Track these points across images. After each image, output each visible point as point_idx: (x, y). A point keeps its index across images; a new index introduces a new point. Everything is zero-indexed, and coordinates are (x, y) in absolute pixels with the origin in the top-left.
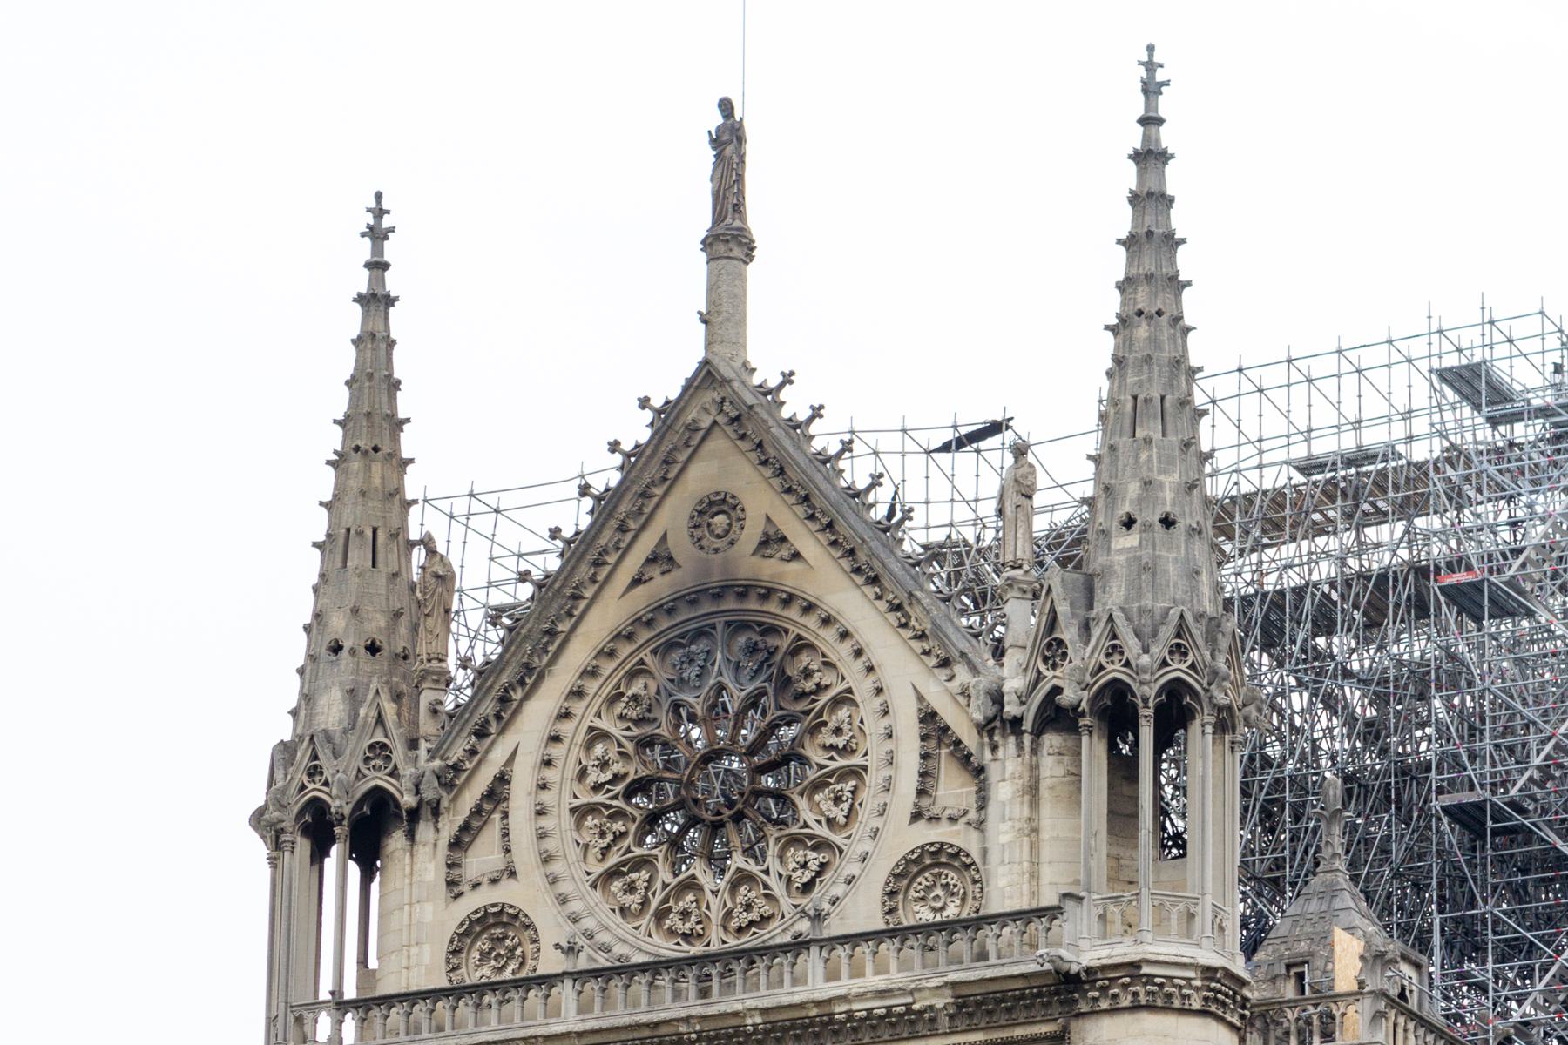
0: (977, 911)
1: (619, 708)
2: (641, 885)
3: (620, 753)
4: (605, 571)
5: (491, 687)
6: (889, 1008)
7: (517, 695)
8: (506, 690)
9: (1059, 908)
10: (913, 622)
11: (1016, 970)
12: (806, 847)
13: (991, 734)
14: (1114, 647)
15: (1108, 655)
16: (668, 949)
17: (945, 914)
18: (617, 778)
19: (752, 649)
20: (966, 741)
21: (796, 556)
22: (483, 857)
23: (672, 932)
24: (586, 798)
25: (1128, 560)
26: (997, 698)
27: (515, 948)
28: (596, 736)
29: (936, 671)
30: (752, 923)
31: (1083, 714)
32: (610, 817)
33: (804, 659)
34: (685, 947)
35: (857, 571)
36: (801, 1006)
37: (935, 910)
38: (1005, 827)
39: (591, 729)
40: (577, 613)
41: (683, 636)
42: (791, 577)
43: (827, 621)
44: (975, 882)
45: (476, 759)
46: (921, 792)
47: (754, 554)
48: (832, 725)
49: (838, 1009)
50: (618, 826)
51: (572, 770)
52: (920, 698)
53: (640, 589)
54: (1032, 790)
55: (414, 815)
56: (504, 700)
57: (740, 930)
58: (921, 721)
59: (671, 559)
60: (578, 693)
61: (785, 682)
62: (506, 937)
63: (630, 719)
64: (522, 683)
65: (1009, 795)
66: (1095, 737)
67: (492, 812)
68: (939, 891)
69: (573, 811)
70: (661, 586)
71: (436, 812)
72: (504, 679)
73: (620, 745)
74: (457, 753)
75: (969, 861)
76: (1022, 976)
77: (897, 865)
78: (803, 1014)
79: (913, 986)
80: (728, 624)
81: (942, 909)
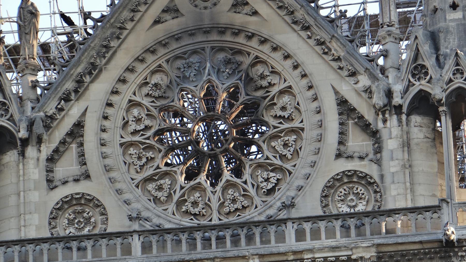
0: (379, 208)
1: (146, 90)
2: (166, 187)
3: (147, 115)
4: (139, 15)
5: (72, 75)
6: (337, 257)
7: (87, 79)
8: (81, 76)
9: (439, 206)
10: (333, 51)
11: (417, 239)
12: (267, 170)
13: (384, 113)
14: (458, 70)
15: (454, 74)
16: (186, 222)
17: (357, 209)
18: (147, 128)
19: (228, 62)
20: (366, 117)
21: (255, 13)
22: (67, 166)
23: (187, 212)
24: (128, 138)
25: (458, 25)
26: (389, 94)
27: (90, 218)
28: (133, 104)
29: (347, 79)
30: (237, 210)
31: (442, 105)
32: (144, 149)
33: (260, 69)
34: (196, 221)
35: (295, 23)
36: (284, 254)
37: (350, 207)
38: (392, 163)
39: (130, 101)
40: (122, 37)
41: (185, 53)
42: (252, 24)
43: (275, 49)
44: (376, 192)
45: (63, 113)
46: (341, 143)
47: (229, 10)
48: (279, 105)
49: (306, 257)
50: (150, 154)
51: (120, 123)
52: (336, 93)
53: (159, 26)
54: (407, 145)
55: (25, 142)
56: (80, 82)
57: (229, 213)
58: (338, 105)
59: (177, 11)
60: (123, 81)
61: (249, 80)
62: (84, 212)
63: (154, 97)
64: (90, 73)
65: (396, 146)
66: (448, 118)
67: (71, 143)
68: (352, 197)
69: (121, 145)
70: (172, 25)
71: (40, 141)
72: (80, 69)
73: (148, 110)
74: (51, 109)
75: (372, 181)
76: (421, 242)
77: (329, 181)
78: (284, 258)
79: (353, 246)
80: (213, 48)
81: (354, 207)
